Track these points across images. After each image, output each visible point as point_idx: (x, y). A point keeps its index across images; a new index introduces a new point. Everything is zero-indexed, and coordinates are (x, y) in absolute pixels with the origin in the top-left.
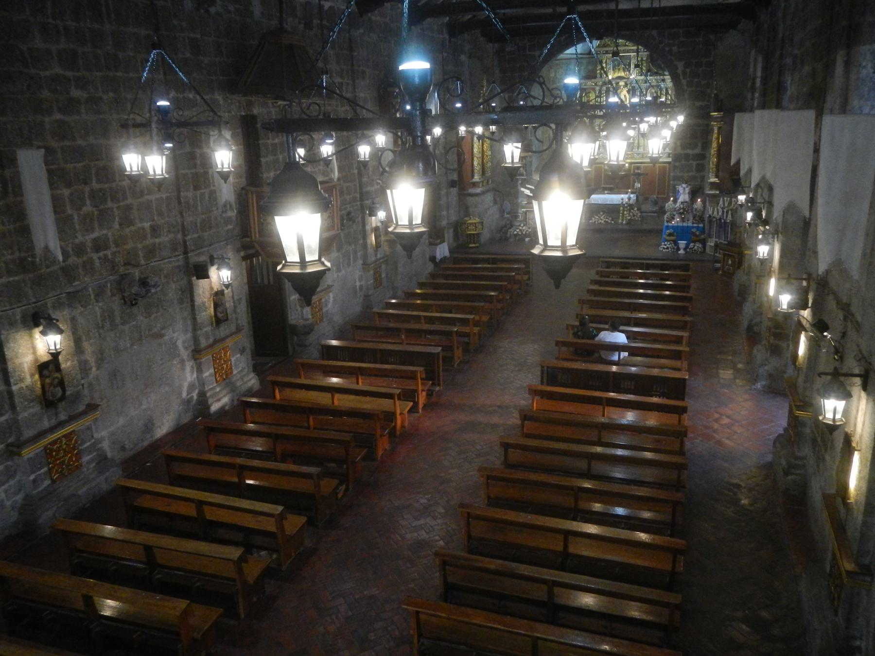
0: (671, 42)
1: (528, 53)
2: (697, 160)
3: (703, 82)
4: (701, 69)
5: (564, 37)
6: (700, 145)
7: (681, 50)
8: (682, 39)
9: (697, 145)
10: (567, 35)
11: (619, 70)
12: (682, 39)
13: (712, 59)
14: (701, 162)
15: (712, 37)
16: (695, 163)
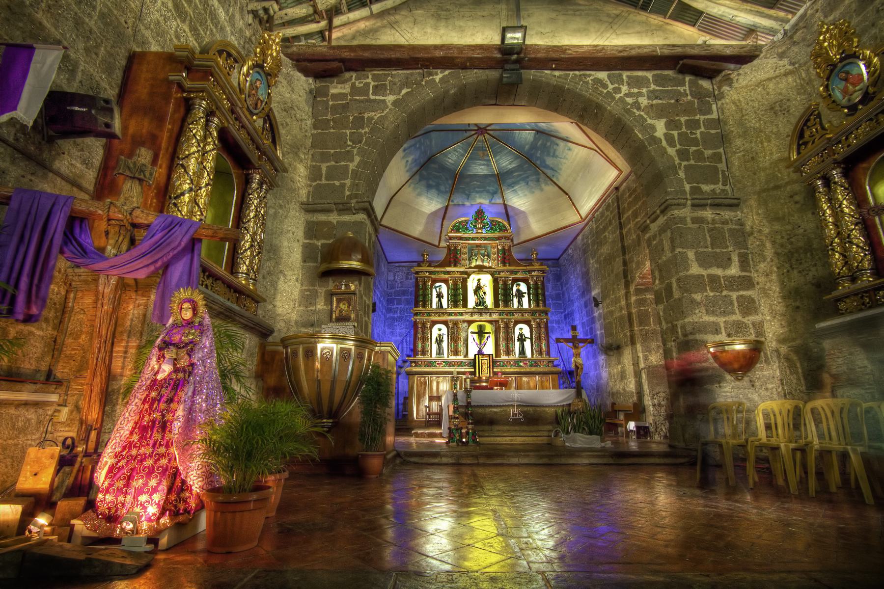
0: (636, 90)
1: (372, 97)
2: (738, 290)
3: (708, 153)
4: (698, 132)
5: (440, 76)
6: (735, 258)
7: (655, 102)
8: (653, 87)
9: (730, 259)
10: (447, 72)
12: (653, 87)
13: (714, 116)
14: (742, 293)
15: (705, 84)
16: (734, 295)
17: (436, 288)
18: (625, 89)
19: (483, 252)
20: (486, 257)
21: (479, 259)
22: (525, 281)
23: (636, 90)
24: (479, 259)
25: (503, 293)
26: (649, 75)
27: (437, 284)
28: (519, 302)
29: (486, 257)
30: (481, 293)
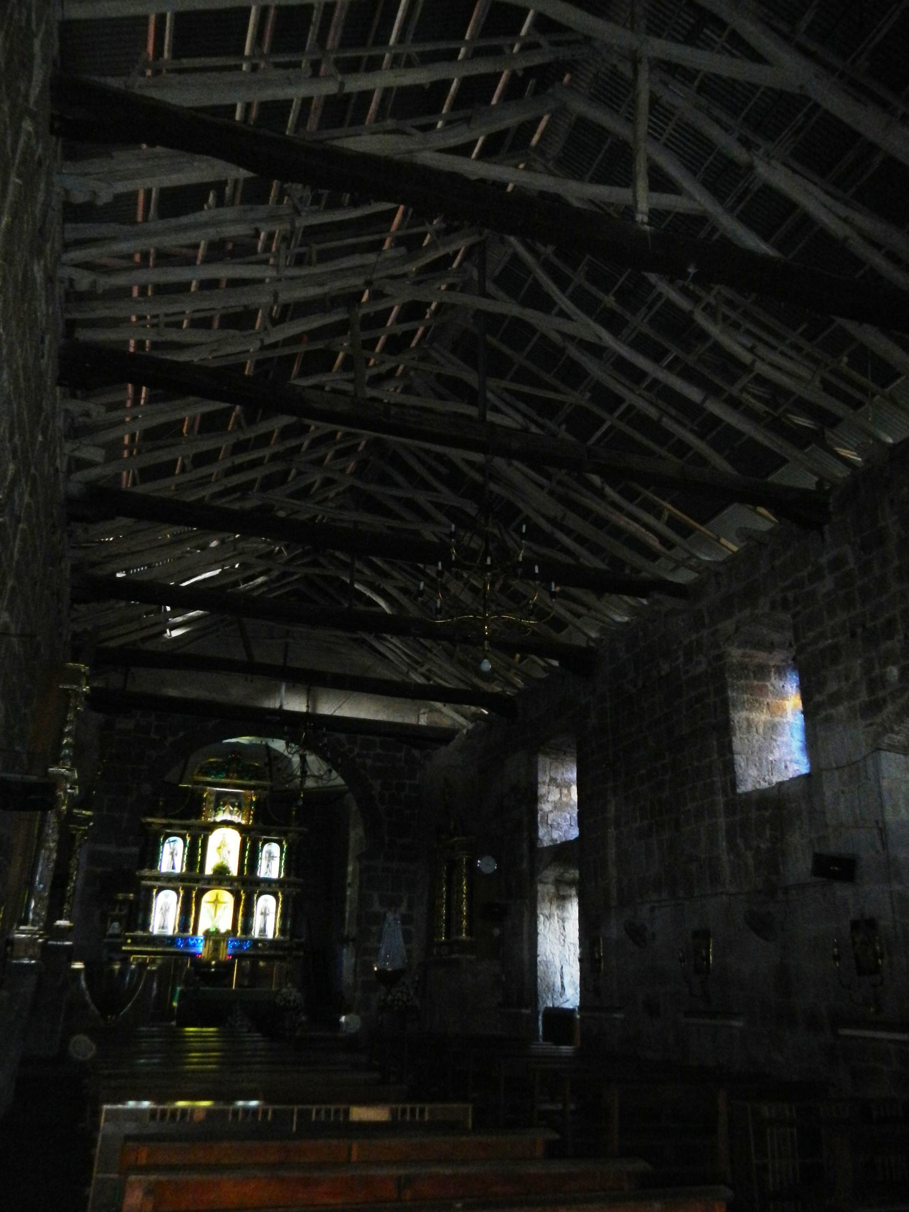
0: (365, 752)
8: (379, 751)
11: (224, 811)
12: (379, 751)
15: (416, 753)
17: (169, 842)
18: (356, 751)
19: (234, 800)
20: (236, 809)
21: (228, 810)
22: (279, 843)
23: (365, 752)
24: (228, 810)
25: (249, 856)
26: (377, 739)
27: (172, 839)
28: (268, 866)
29: (236, 809)
30: (224, 851)
